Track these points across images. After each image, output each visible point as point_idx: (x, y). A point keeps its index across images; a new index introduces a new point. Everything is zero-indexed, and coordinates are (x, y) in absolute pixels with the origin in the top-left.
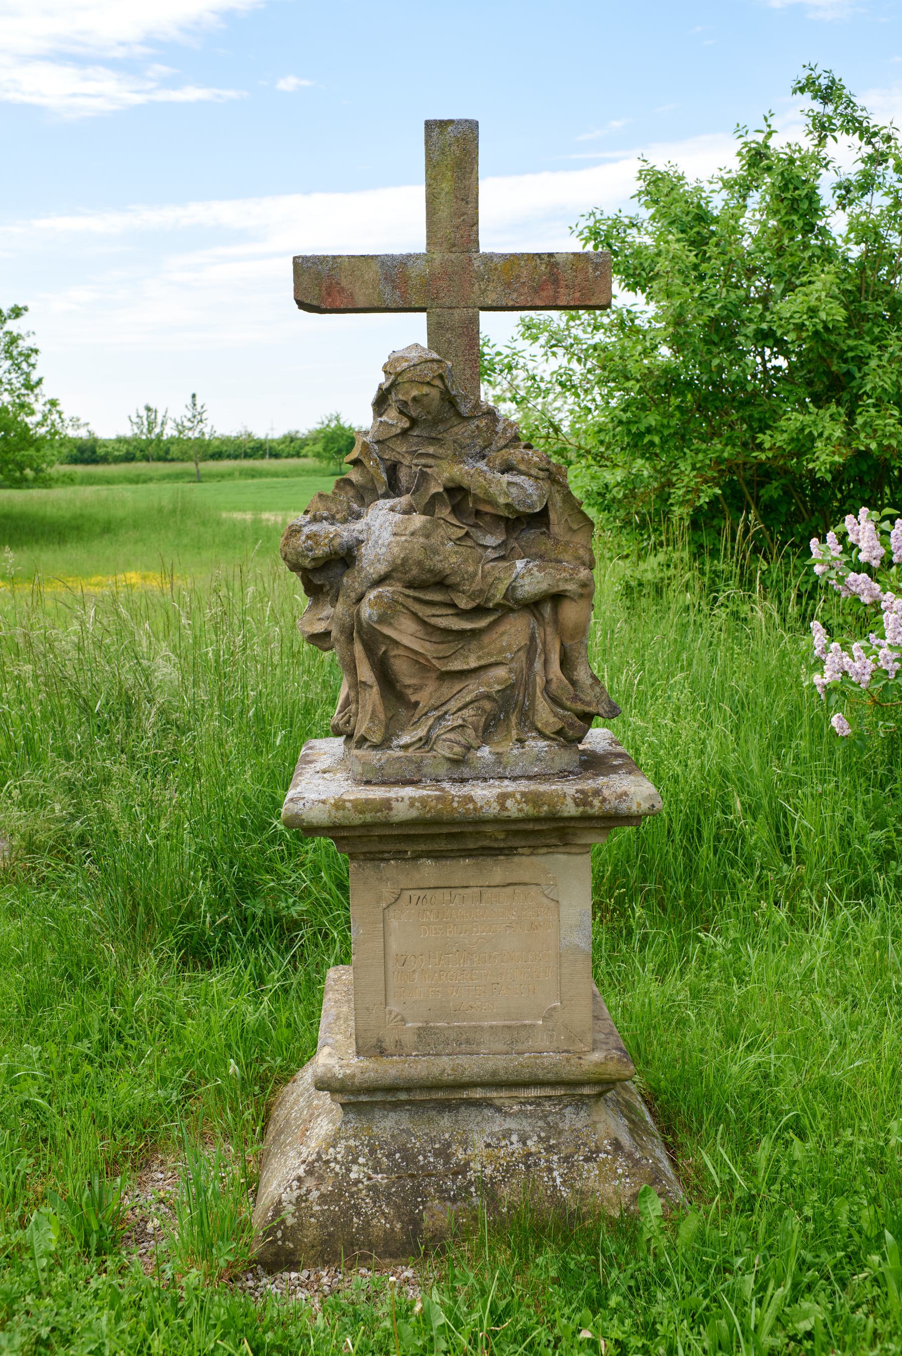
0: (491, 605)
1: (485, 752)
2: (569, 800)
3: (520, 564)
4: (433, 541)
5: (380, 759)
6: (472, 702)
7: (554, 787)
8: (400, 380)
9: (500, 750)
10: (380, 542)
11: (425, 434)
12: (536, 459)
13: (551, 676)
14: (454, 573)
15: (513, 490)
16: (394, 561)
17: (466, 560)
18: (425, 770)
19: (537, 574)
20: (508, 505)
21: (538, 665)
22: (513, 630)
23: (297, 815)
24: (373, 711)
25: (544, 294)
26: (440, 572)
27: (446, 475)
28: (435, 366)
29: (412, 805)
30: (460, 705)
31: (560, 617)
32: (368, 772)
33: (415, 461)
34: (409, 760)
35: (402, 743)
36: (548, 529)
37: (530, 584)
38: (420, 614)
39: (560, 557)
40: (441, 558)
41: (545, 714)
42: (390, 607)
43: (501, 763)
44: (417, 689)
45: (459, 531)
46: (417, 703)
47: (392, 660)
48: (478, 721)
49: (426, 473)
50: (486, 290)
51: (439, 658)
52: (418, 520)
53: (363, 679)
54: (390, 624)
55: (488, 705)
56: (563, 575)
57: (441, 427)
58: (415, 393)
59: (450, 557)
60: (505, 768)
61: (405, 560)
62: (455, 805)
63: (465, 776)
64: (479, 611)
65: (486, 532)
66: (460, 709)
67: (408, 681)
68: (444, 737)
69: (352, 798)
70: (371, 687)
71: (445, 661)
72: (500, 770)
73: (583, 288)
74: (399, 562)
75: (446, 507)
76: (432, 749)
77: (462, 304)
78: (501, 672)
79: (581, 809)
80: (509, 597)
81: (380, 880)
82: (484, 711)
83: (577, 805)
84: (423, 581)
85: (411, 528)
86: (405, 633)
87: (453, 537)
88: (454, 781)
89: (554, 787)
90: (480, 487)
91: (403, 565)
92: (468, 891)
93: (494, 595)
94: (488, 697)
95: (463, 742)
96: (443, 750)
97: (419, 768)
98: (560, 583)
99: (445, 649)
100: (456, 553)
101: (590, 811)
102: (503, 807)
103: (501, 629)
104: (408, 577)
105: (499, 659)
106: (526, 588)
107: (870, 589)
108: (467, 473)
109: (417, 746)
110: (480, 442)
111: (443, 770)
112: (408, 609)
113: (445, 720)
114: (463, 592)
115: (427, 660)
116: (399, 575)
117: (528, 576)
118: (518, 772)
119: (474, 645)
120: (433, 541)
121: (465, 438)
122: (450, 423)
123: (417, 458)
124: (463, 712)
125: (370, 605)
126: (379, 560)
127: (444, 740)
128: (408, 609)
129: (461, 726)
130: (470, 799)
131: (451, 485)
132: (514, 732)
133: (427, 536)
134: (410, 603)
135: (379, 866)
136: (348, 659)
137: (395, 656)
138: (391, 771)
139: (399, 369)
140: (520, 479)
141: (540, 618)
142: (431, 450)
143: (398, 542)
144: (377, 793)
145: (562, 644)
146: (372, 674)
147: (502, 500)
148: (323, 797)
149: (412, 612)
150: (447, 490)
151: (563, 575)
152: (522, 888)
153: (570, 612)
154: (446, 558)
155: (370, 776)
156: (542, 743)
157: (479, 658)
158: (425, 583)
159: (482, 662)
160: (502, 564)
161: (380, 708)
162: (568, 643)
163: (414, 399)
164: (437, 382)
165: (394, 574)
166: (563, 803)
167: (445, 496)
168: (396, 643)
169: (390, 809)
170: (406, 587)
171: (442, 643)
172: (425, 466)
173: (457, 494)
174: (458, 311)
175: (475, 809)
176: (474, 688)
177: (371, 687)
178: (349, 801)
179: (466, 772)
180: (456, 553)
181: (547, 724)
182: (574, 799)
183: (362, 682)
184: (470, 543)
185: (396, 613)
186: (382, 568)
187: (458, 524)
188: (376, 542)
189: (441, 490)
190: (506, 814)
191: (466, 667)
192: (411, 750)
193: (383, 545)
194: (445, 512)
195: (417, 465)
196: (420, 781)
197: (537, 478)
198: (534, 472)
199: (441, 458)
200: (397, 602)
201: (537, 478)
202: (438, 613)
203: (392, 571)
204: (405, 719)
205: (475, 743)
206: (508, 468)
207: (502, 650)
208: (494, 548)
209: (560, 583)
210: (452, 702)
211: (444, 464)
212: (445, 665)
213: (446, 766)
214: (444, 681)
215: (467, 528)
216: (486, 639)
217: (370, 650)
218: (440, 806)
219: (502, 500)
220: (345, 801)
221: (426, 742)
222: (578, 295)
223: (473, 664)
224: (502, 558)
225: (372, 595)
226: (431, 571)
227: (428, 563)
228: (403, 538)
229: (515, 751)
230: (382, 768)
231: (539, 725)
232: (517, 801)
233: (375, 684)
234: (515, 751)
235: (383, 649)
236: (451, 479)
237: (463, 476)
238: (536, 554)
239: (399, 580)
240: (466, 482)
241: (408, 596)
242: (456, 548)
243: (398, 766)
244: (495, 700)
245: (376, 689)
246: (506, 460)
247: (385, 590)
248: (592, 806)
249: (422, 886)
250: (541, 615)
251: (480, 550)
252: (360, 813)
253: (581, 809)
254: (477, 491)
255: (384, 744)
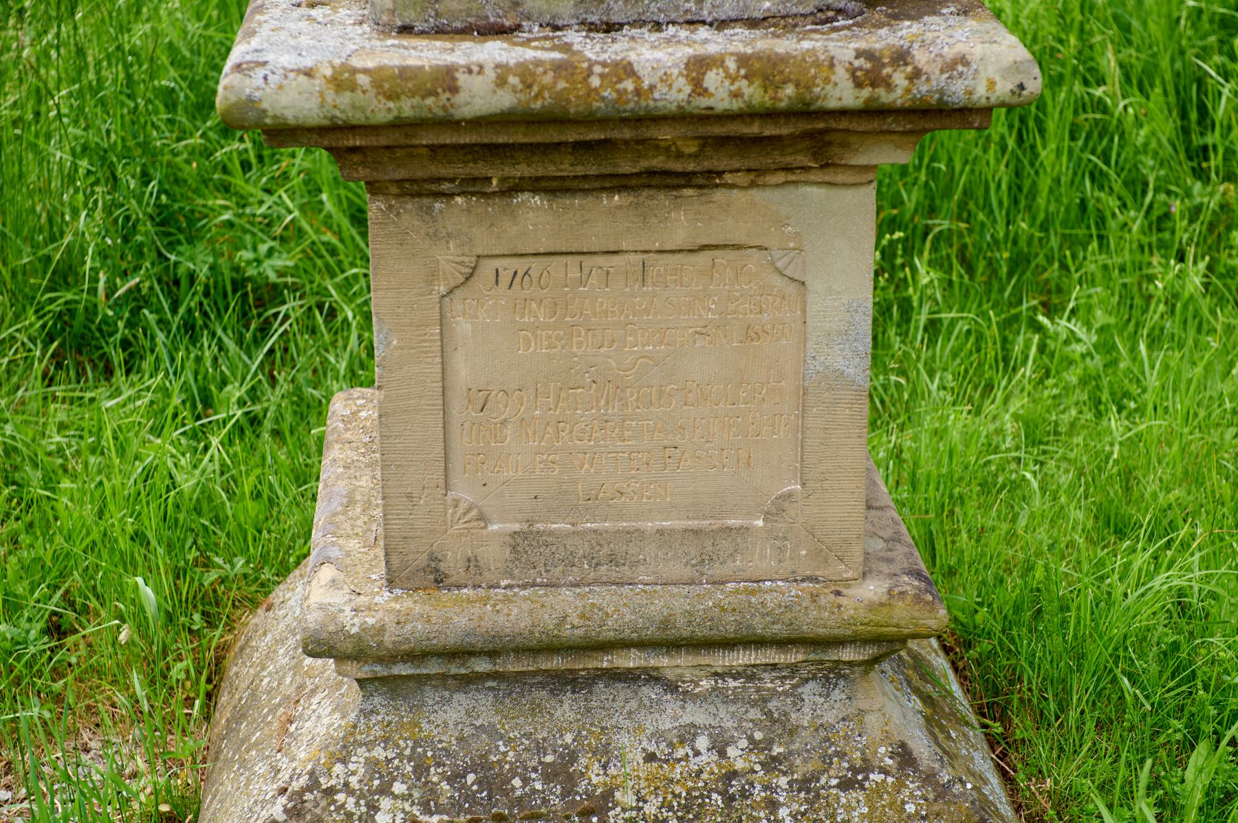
2: (841, 75)
7: (806, 45)
23: (250, 102)
29: (501, 82)
62: (595, 82)
63: (615, 18)
69: (370, 64)
79: (866, 92)
83: (859, 85)
88: (592, 28)
89: (806, 45)
92: (616, 260)
101: (884, 97)
102: (699, 88)
118: (728, 11)
130: (627, 70)
135: (430, 208)
144: (426, 54)
148: (308, 62)
152: (731, 255)
166: (827, 80)
169: (454, 89)
175: (638, 92)
178: (365, 71)
182: (853, 72)
190: (704, 102)
196: (518, 27)
218: (562, 85)
220: (354, 71)
232: (728, 75)
248: (889, 85)
253: (866, 92)
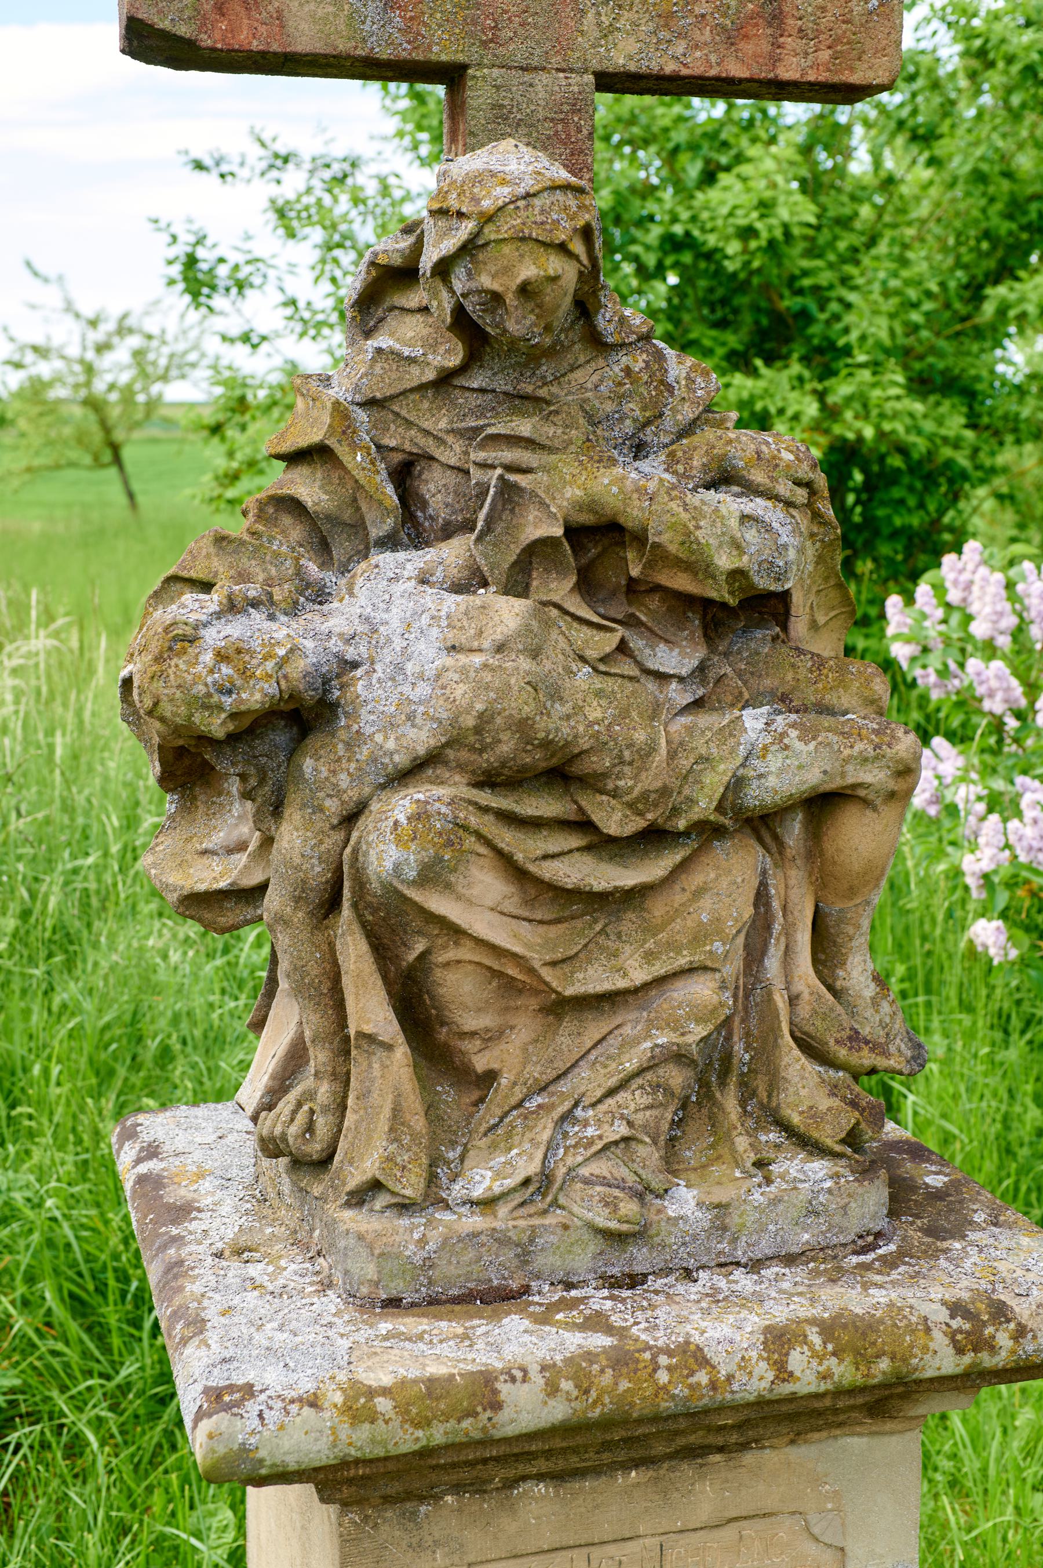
0: (682, 824)
1: (685, 1202)
2: (940, 1340)
3: (753, 720)
4: (548, 665)
5: (423, 1242)
6: (640, 1072)
7: (880, 1296)
8: (490, 233)
9: (721, 1195)
10: (409, 667)
11: (501, 384)
12: (787, 456)
13: (799, 987)
14: (599, 747)
15: (751, 535)
16: (454, 721)
17: (624, 714)
18: (541, 1261)
19: (799, 745)
20: (737, 575)
21: (773, 964)
22: (724, 883)
23: (244, 1449)
24: (397, 1112)
25: (747, 48)
26: (567, 744)
27: (573, 493)
28: (571, 201)
29: (552, 1389)
30: (613, 1082)
31: (829, 848)
32: (392, 1276)
33: (481, 456)
34: (502, 1240)
35: (477, 1193)
36: (785, 628)
37: (781, 771)
38: (519, 857)
39: (831, 699)
40: (567, 709)
41: (804, 1088)
42: (450, 843)
43: (724, 1228)
44: (490, 1038)
45: (598, 636)
46: (491, 1077)
47: (438, 974)
48: (658, 1120)
49: (515, 487)
50: (612, 29)
51: (554, 964)
52: (508, 613)
53: (368, 1029)
54: (448, 886)
55: (677, 1077)
56: (859, 746)
57: (546, 369)
58: (528, 271)
59: (587, 709)
60: (734, 1240)
61: (485, 719)
62: (663, 1377)
63: (638, 1269)
64: (654, 837)
65: (654, 636)
66: (611, 1093)
67: (471, 1022)
68: (585, 1171)
69: (387, 1380)
70: (389, 1047)
71: (567, 968)
72: (724, 1246)
73: (838, 40)
74: (470, 722)
75: (562, 571)
76: (555, 1203)
77: (556, 61)
78: (702, 990)
79: (968, 1359)
80: (728, 804)
81: (418, 1547)
82: (669, 1092)
83: (960, 1351)
84: (524, 769)
85: (497, 633)
86: (480, 905)
87: (592, 654)
88: (613, 1283)
89: (880, 1296)
90: (673, 527)
91: (478, 730)
92: (631, 1547)
93: (691, 801)
94: (678, 1057)
95: (631, 1179)
96: (588, 1209)
97: (524, 1257)
98: (850, 768)
99: (564, 939)
100: (599, 694)
101: (987, 1360)
102: (783, 1373)
103: (696, 879)
104: (488, 759)
105: (698, 958)
106: (772, 781)
107: (1008, 689)
108: (641, 491)
109: (518, 1198)
110: (633, 408)
111: (583, 1258)
112: (488, 843)
113: (576, 1121)
114: (615, 794)
115: (531, 971)
116: (464, 755)
117: (772, 751)
118: (765, 1247)
119: (629, 922)
120: (548, 665)
121: (602, 399)
122: (570, 358)
123: (482, 446)
124: (621, 1097)
125: (398, 841)
126: (410, 717)
127: (587, 1182)
128: (488, 843)
129: (626, 1140)
130: (693, 1357)
131: (585, 518)
132: (742, 1143)
133: (535, 654)
134: (490, 827)
135: (414, 1513)
136: (314, 970)
137: (447, 965)
138: (452, 1270)
139: (487, 204)
140: (758, 506)
141: (775, 846)
142: (524, 427)
143: (464, 671)
144: (440, 1351)
145: (817, 906)
146: (391, 1015)
147: (724, 561)
148: (306, 1386)
149: (499, 853)
150: (572, 531)
151: (859, 746)
152: (759, 1524)
153: (855, 835)
154: (578, 709)
155: (396, 1287)
156: (819, 1168)
157: (650, 957)
158: (532, 774)
159: (660, 969)
160: (704, 720)
161: (413, 1103)
162: (834, 906)
163: (525, 290)
164: (578, 247)
165: (451, 754)
166: (925, 1349)
167: (567, 546)
168: (456, 932)
169: (496, 1406)
170: (478, 785)
171: (558, 921)
172: (509, 468)
173: (597, 542)
174: (544, 78)
175: (713, 1385)
176: (638, 1039)
177: (389, 1047)
178: (385, 1392)
179: (641, 1258)
180: (599, 694)
181: (812, 1113)
182: (952, 1335)
183: (360, 1035)
184: (628, 668)
185: (462, 856)
186: (421, 739)
187: (596, 619)
188: (399, 668)
189: (558, 531)
190: (787, 1389)
191: (622, 984)
192: (503, 1210)
193: (421, 676)
194: (560, 588)
195: (484, 466)
196: (526, 1290)
197: (789, 504)
198: (784, 488)
199: (550, 450)
200: (465, 828)
201: (789, 504)
202: (553, 848)
203: (448, 744)
204: (456, 1115)
205: (657, 1182)
206: (723, 478)
207: (699, 937)
208: (681, 679)
209: (850, 768)
210: (584, 1071)
211: (566, 465)
212: (569, 979)
213: (594, 1245)
214: (559, 1018)
215: (621, 631)
216: (658, 908)
217: (382, 950)
218: (624, 1385)
219: (724, 561)
220: (371, 1393)
221: (540, 1186)
222: (825, 55)
223: (639, 976)
224: (698, 704)
225: (401, 806)
226: (546, 744)
227: (543, 727)
228: (477, 659)
229: (757, 1196)
230: (428, 1263)
231: (796, 1119)
232: (815, 1354)
233: (401, 1039)
234: (757, 1196)
235: (420, 947)
236: (590, 505)
237: (627, 500)
238: (772, 692)
239: (461, 767)
240: (634, 514)
241: (485, 810)
242: (598, 682)
243: (471, 1254)
244: (693, 1063)
245: (402, 1052)
246: (723, 457)
247: (440, 794)
248: (993, 1349)
249: (521, 1548)
250: (776, 838)
251: (651, 685)
252: (417, 1426)
253: (968, 1359)
254: (664, 539)
255: (433, 1198)
